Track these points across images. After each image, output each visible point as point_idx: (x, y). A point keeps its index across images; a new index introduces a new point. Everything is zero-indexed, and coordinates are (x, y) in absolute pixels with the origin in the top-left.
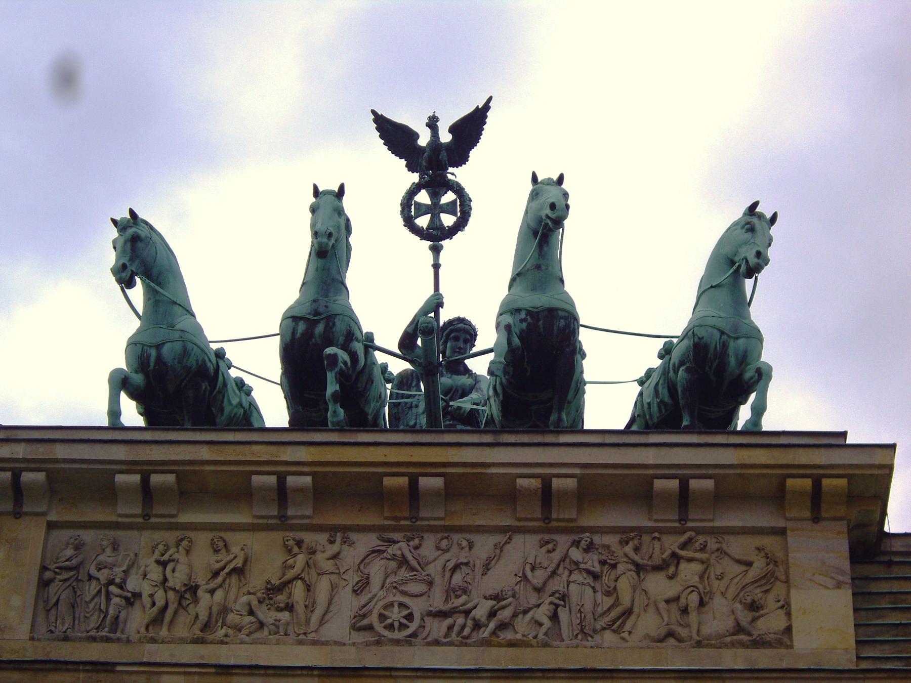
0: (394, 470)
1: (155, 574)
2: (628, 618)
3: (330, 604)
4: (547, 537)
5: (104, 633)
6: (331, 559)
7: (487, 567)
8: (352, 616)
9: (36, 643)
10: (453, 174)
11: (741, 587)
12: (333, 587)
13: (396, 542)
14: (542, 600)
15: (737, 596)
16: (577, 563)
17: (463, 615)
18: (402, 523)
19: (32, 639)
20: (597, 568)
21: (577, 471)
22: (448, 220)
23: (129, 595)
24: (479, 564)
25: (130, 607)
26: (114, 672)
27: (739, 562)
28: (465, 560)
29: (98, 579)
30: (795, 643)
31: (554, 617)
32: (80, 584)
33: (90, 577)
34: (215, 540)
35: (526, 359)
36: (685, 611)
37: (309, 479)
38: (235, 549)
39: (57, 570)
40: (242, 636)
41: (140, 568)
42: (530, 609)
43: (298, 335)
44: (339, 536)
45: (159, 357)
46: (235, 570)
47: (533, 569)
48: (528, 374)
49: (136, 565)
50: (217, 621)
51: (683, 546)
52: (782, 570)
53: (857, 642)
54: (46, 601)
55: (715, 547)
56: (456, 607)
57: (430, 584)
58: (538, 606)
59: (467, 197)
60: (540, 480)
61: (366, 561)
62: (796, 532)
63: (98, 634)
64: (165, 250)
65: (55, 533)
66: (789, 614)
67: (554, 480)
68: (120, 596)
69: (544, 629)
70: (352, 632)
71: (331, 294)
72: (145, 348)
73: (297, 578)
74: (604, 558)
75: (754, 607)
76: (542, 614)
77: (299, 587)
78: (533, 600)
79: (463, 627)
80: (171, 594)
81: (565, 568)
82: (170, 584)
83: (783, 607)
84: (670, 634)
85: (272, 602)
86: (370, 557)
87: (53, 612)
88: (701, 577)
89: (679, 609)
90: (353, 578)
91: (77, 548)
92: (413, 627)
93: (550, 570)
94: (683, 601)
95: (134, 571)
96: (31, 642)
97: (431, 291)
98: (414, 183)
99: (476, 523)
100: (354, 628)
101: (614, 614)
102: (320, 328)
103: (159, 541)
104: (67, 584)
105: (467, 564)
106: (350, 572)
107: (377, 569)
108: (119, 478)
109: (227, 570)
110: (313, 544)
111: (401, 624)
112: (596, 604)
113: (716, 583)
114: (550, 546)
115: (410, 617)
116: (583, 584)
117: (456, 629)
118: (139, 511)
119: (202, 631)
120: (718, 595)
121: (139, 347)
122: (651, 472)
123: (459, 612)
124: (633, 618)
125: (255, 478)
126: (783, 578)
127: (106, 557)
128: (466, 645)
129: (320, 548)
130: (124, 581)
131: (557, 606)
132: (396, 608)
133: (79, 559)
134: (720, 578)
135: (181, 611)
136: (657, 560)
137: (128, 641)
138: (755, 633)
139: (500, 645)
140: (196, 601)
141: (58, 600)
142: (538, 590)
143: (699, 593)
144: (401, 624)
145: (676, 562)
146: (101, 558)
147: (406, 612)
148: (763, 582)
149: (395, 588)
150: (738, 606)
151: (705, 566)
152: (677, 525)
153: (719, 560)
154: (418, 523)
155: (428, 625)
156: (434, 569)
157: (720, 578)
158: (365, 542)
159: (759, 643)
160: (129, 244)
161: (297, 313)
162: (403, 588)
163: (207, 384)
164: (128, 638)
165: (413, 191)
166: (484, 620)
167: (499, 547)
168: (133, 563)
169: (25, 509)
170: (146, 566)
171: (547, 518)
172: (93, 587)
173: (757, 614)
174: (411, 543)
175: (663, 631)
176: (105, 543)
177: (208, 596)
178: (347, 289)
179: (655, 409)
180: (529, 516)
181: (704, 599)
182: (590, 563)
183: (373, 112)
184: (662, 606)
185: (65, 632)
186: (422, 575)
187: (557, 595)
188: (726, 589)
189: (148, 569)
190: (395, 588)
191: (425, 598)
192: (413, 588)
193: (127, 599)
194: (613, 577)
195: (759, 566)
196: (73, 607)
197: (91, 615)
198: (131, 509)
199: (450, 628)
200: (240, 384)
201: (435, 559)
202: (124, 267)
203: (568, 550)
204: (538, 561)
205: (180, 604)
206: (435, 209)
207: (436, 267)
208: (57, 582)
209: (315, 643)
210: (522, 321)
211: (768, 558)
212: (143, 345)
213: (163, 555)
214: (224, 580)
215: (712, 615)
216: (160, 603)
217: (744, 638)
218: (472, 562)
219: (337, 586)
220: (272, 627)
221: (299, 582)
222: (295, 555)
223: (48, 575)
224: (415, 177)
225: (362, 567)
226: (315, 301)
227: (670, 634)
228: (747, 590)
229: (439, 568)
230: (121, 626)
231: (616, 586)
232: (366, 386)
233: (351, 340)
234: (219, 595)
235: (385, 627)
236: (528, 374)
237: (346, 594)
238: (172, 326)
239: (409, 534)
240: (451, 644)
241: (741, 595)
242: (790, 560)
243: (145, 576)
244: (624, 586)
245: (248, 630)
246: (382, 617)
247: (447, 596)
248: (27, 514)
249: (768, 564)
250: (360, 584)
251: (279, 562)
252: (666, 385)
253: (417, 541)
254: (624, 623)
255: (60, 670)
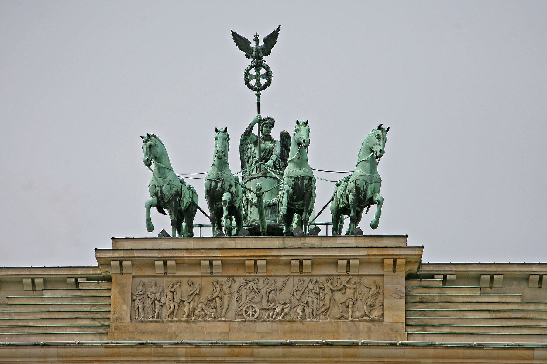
0: (249, 258)
1: (170, 296)
2: (328, 310)
3: (229, 305)
4: (301, 278)
5: (154, 319)
6: (228, 288)
7: (281, 290)
8: (236, 310)
9: (133, 323)
10: (265, 61)
11: (367, 298)
12: (229, 299)
13: (250, 282)
14: (299, 304)
15: (366, 301)
16: (311, 290)
17: (273, 310)
18: (252, 274)
19: (131, 322)
20: (318, 292)
21: (312, 258)
22: (263, 81)
23: (162, 304)
24: (278, 289)
25: (162, 308)
26: (163, 347)
27: (367, 287)
28: (273, 289)
29: (151, 298)
30: (384, 320)
31: (303, 310)
32: (145, 299)
33: (148, 297)
34: (189, 282)
35: (294, 194)
36: (348, 307)
37: (220, 262)
38: (196, 286)
39: (137, 295)
40: (200, 319)
41: (165, 293)
42: (296, 307)
43: (212, 187)
44: (231, 279)
45: (161, 191)
46: (197, 294)
47: (296, 291)
48: (295, 198)
49: (163, 292)
50: (192, 313)
51: (347, 283)
52: (381, 290)
53: (406, 318)
54: (134, 307)
55: (359, 281)
56: (271, 308)
57: (262, 297)
58: (299, 305)
59: (270, 72)
60: (299, 261)
61: (240, 289)
62: (387, 276)
63: (153, 320)
64: (160, 144)
65: (135, 279)
66: (383, 309)
67: (304, 261)
68: (160, 305)
69: (300, 316)
70: (236, 316)
71: (223, 170)
72: (156, 187)
73: (217, 296)
74: (321, 287)
75: (371, 306)
76: (299, 310)
77: (218, 300)
78: (297, 304)
79: (273, 315)
80: (176, 304)
81: (307, 290)
82: (175, 300)
83: (381, 305)
84: (342, 316)
85: (209, 305)
86: (241, 287)
87: (137, 310)
88: (354, 294)
89: (346, 306)
90: (236, 295)
91: (143, 286)
92: (257, 315)
93: (302, 291)
94: (347, 304)
95: (162, 294)
96: (131, 323)
97: (257, 115)
98: (249, 65)
99: (277, 274)
100: (236, 314)
101: (323, 309)
102: (219, 185)
103: (170, 283)
104: (141, 301)
105: (274, 290)
106: (235, 292)
107: (244, 293)
108: (156, 262)
109: (194, 294)
110: (222, 283)
111: (252, 314)
112: (317, 305)
113: (358, 296)
114: (302, 282)
115: (255, 312)
116: (313, 297)
117: (271, 315)
118: (163, 272)
119: (187, 318)
120: (359, 300)
121: (154, 187)
122: (337, 258)
123: (272, 309)
124: (330, 310)
125: (202, 261)
126: (382, 294)
127: (153, 290)
128: (274, 322)
129: (224, 284)
130: (160, 299)
131: (304, 306)
132: (251, 308)
133: (144, 290)
134: (360, 294)
135: (180, 309)
136: (339, 289)
137: (163, 322)
138: (371, 317)
139: (285, 322)
140: (184, 306)
141: (138, 307)
142: (298, 300)
143: (353, 301)
144: (252, 314)
145: (345, 288)
146: (151, 290)
147: (254, 310)
148: (375, 295)
149: (250, 300)
150: (365, 307)
151: (355, 289)
152: (346, 274)
153: (360, 287)
154: (258, 274)
155: (261, 313)
156: (263, 291)
157: (360, 294)
158: (241, 280)
159: (372, 321)
160: (148, 149)
161: (211, 178)
162: (253, 300)
163: (179, 197)
164: (163, 321)
165: (248, 70)
166: (280, 312)
167: (285, 283)
168: (162, 292)
169: (124, 272)
170: (167, 293)
171: (301, 272)
172: (149, 302)
173: (372, 309)
174: (255, 282)
175: (339, 316)
176: (152, 284)
177: (188, 304)
178: (229, 164)
179: (341, 201)
180: (295, 272)
181: (354, 302)
182: (315, 289)
183: (232, 31)
184: (340, 305)
185: (142, 319)
186: (259, 295)
187: (304, 303)
188: (362, 298)
189: (168, 294)
190: (250, 300)
191: (260, 303)
192: (256, 300)
193: (161, 305)
194: (323, 294)
195: (374, 289)
196: (143, 309)
197: (150, 312)
198: (160, 271)
199: (269, 315)
200: (190, 188)
201: (263, 288)
202: (148, 159)
203: (308, 284)
204: (298, 288)
205: (179, 306)
206: (258, 77)
207: (259, 103)
208: (137, 299)
209: (224, 321)
210: (293, 181)
211: (377, 286)
212: (155, 186)
213: (172, 288)
214: (193, 298)
215: (357, 308)
216: (172, 308)
217: (366, 318)
218: (276, 289)
219: (231, 298)
220: (210, 316)
221: (218, 297)
222: (216, 288)
223: (134, 298)
224: (249, 61)
225: (239, 291)
226: (217, 173)
227: (342, 316)
228: (369, 299)
229: (265, 291)
230: (160, 315)
231: (324, 298)
232: (236, 200)
233: (231, 187)
234: (192, 303)
235: (247, 315)
236: (295, 198)
237: (234, 301)
238: (165, 178)
239: (254, 277)
240: (269, 321)
241: (367, 301)
242: (385, 288)
243: (167, 296)
244: (327, 298)
245: (202, 317)
246: (246, 312)
247: (267, 303)
248: (125, 273)
249: (377, 289)
250: (238, 298)
251: (211, 290)
252: (345, 195)
253: (257, 281)
254: (327, 312)
255: (146, 347)
